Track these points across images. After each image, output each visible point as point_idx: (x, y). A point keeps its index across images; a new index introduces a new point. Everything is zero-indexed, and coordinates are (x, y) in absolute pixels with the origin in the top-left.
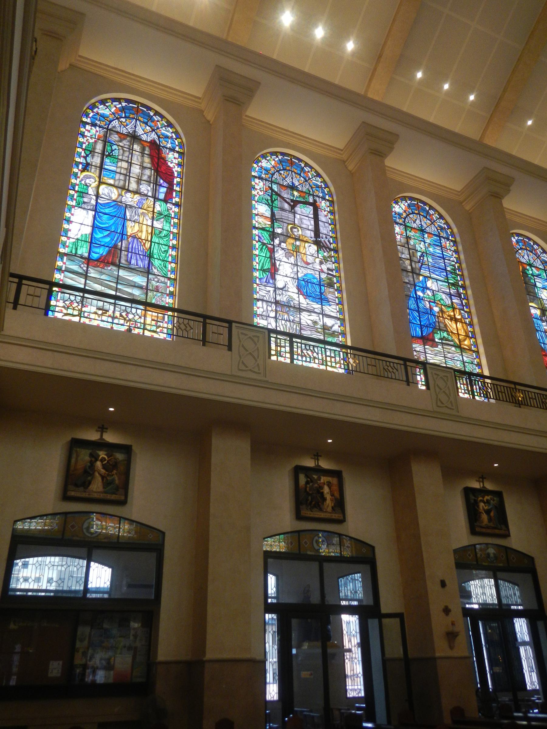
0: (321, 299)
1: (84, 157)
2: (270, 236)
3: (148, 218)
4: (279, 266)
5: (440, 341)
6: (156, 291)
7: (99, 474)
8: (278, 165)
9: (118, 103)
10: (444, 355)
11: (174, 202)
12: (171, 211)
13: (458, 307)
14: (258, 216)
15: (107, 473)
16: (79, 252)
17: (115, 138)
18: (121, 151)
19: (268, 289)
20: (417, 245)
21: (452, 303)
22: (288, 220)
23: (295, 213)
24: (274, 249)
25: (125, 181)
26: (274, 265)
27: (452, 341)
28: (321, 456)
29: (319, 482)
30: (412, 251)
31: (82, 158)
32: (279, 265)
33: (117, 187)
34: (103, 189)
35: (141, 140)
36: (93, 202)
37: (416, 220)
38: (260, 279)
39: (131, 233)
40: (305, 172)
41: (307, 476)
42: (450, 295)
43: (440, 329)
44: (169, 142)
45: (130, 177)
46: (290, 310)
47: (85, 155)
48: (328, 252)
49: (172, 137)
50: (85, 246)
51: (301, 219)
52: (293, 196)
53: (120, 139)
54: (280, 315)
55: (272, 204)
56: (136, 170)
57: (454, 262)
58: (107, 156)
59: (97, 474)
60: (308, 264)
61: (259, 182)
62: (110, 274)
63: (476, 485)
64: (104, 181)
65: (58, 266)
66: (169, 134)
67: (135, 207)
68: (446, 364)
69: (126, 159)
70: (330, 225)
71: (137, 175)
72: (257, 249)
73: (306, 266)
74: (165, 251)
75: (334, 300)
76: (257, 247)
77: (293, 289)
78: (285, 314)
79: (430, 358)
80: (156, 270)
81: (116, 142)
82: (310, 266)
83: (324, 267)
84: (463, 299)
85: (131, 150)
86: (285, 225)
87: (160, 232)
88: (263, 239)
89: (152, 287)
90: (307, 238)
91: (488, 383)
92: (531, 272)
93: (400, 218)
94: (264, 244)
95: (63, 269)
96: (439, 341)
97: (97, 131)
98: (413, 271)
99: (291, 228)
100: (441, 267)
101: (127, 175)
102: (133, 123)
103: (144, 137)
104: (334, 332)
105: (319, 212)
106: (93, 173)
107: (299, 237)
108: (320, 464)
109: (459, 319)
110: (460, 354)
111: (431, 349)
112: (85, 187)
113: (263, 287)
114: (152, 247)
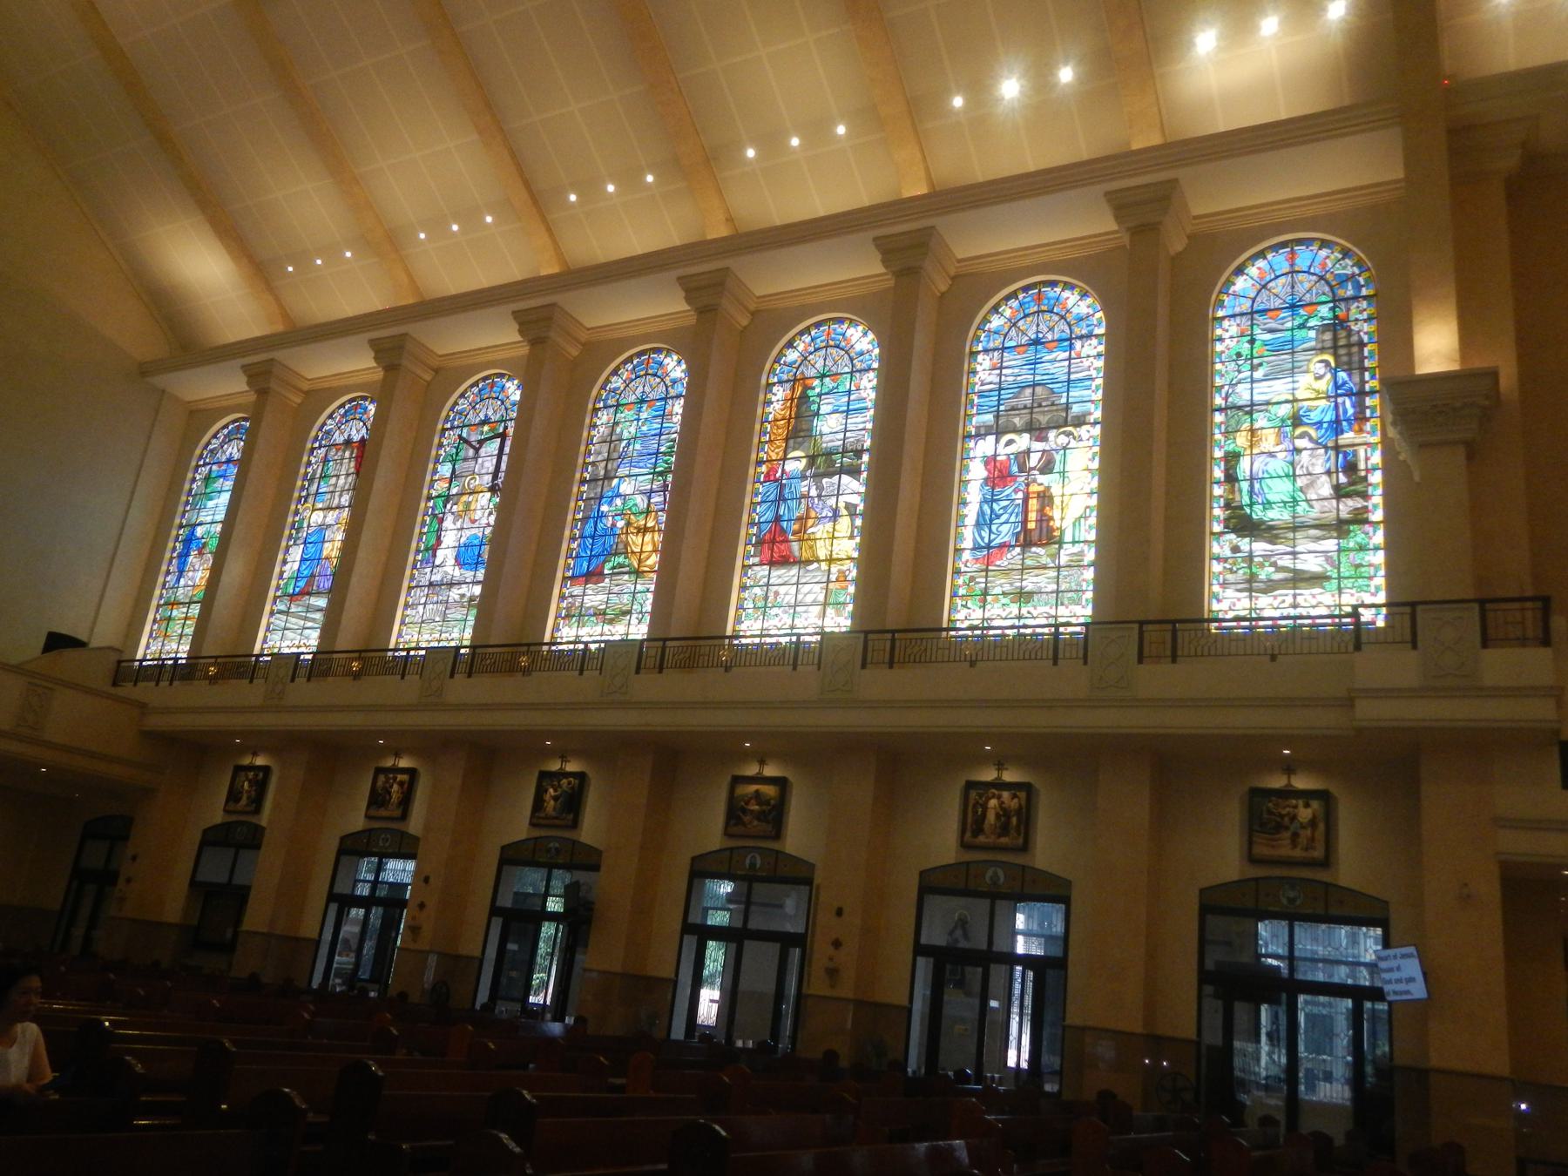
21: (649, 505)
27: (628, 566)
43: (616, 554)
52: (482, 433)
82: (476, 525)
92: (818, 390)
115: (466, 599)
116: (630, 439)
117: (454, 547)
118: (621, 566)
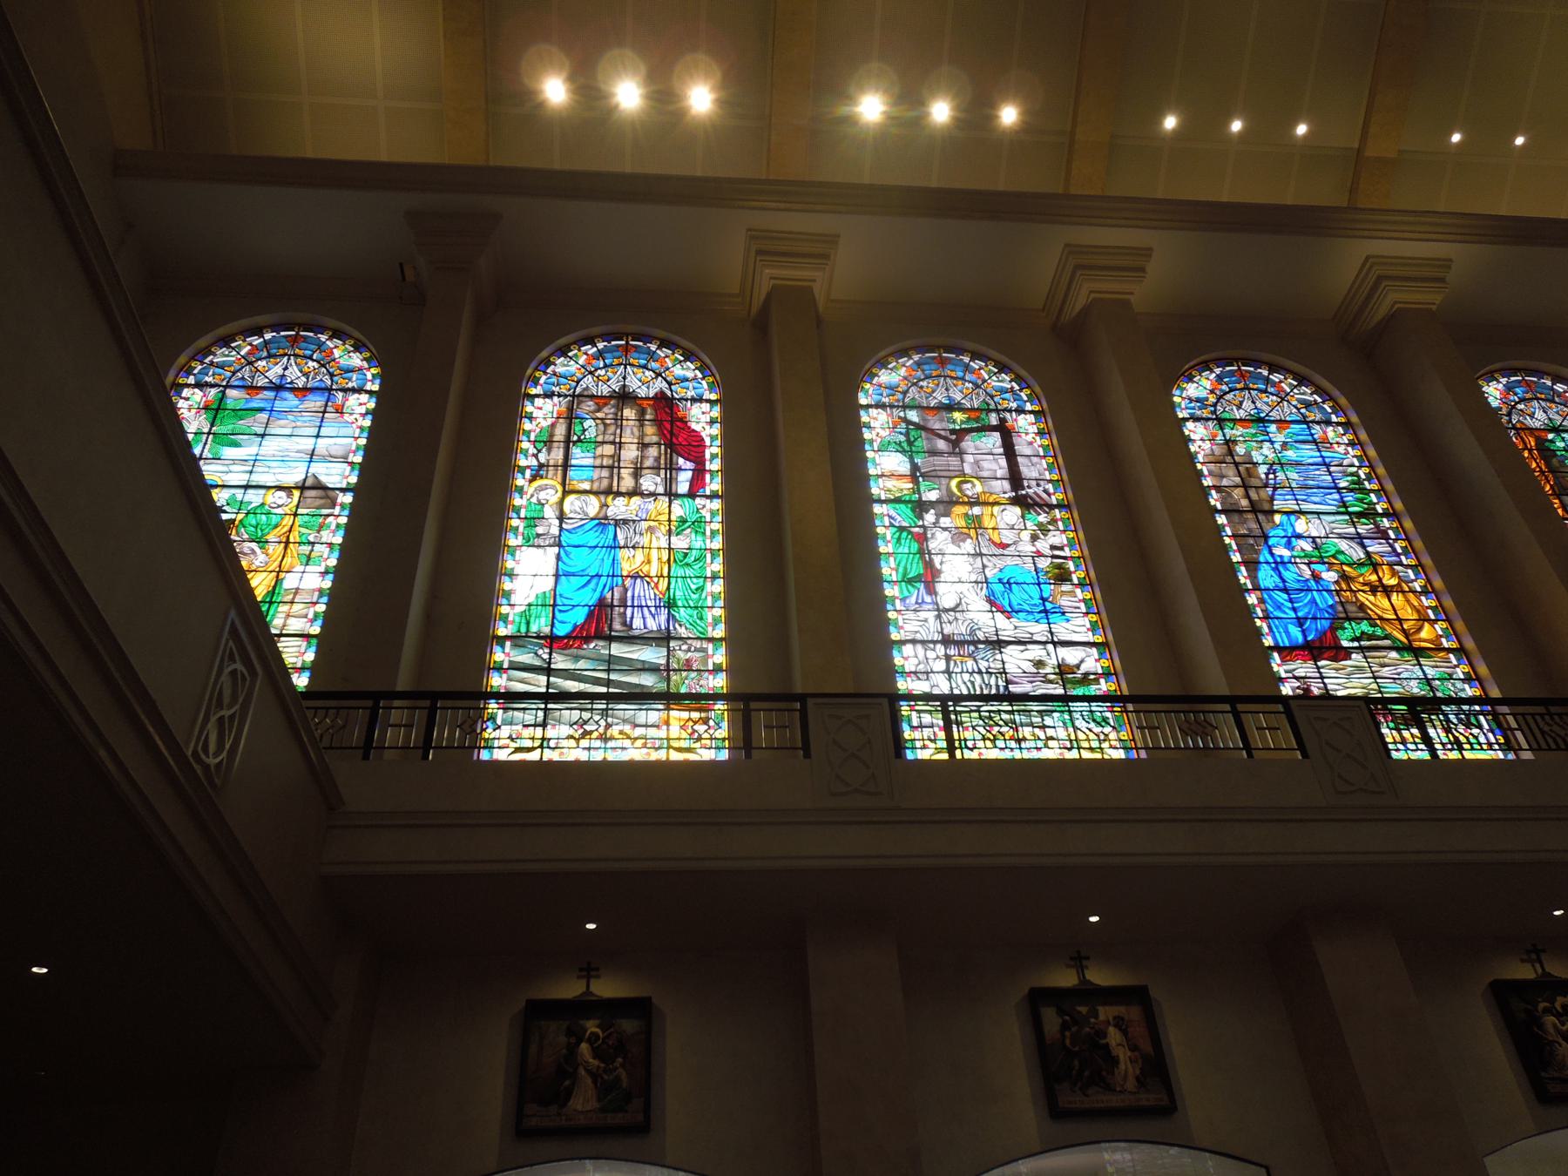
0: (1046, 611)
1: (533, 455)
2: (913, 510)
3: (660, 535)
4: (941, 564)
5: (1356, 644)
6: (685, 670)
7: (585, 1069)
8: (913, 373)
9: (590, 346)
10: (1372, 672)
11: (708, 493)
12: (703, 512)
13: (1386, 560)
14: (884, 478)
15: (602, 1065)
16: (534, 628)
17: (587, 408)
18: (601, 427)
19: (922, 615)
20: (1253, 453)
21: (1368, 554)
22: (949, 470)
23: (961, 453)
24: (925, 533)
25: (611, 477)
26: (929, 565)
27: (1386, 637)
28: (1088, 958)
29: (1092, 1020)
30: (1246, 468)
31: (530, 458)
32: (941, 563)
33: (596, 493)
34: (571, 503)
35: (636, 398)
36: (555, 531)
37: (1241, 403)
38: (903, 600)
39: (630, 569)
40: (973, 371)
41: (1061, 1012)
42: (1359, 539)
43: (1349, 619)
44: (691, 388)
45: (619, 468)
46: (977, 648)
47: (535, 452)
48: (1047, 513)
49: (695, 378)
50: (543, 613)
51: (977, 462)
52: (954, 422)
53: (596, 407)
54: (955, 663)
55: (911, 448)
56: (630, 453)
57: (1354, 466)
58: (575, 443)
59: (582, 1072)
60: (1004, 546)
61: (879, 413)
62: (593, 656)
63: (1526, 972)
64: (571, 487)
65: (495, 662)
66: (690, 375)
67: (634, 521)
68: (1380, 692)
69: (612, 438)
70: (1044, 457)
71: (632, 463)
72: (889, 542)
73: (1001, 551)
74: (697, 589)
75: (1076, 608)
76: (889, 538)
77: (977, 605)
78: (966, 659)
79: (1337, 687)
80: (683, 628)
81: (591, 414)
83: (1043, 545)
84: (1395, 540)
85: (619, 420)
86: (944, 481)
87: (686, 554)
88: (899, 519)
89: (679, 664)
90: (995, 496)
91: (1504, 715)
93: (1205, 407)
94: (902, 529)
95: (506, 666)
96: (1351, 644)
97: (555, 405)
98: (1255, 509)
99: (959, 485)
100: (1324, 485)
101: (614, 467)
102: (619, 373)
103: (642, 392)
104: (1086, 674)
105: (1015, 440)
106: (552, 481)
107: (978, 498)
108: (1088, 977)
109: (1393, 586)
110: (1416, 662)
111: (1335, 665)
112: (539, 507)
113: (910, 615)
114: (672, 586)
115: (1048, 670)
116: (1272, 465)
117: (976, 582)
118: (1364, 636)
